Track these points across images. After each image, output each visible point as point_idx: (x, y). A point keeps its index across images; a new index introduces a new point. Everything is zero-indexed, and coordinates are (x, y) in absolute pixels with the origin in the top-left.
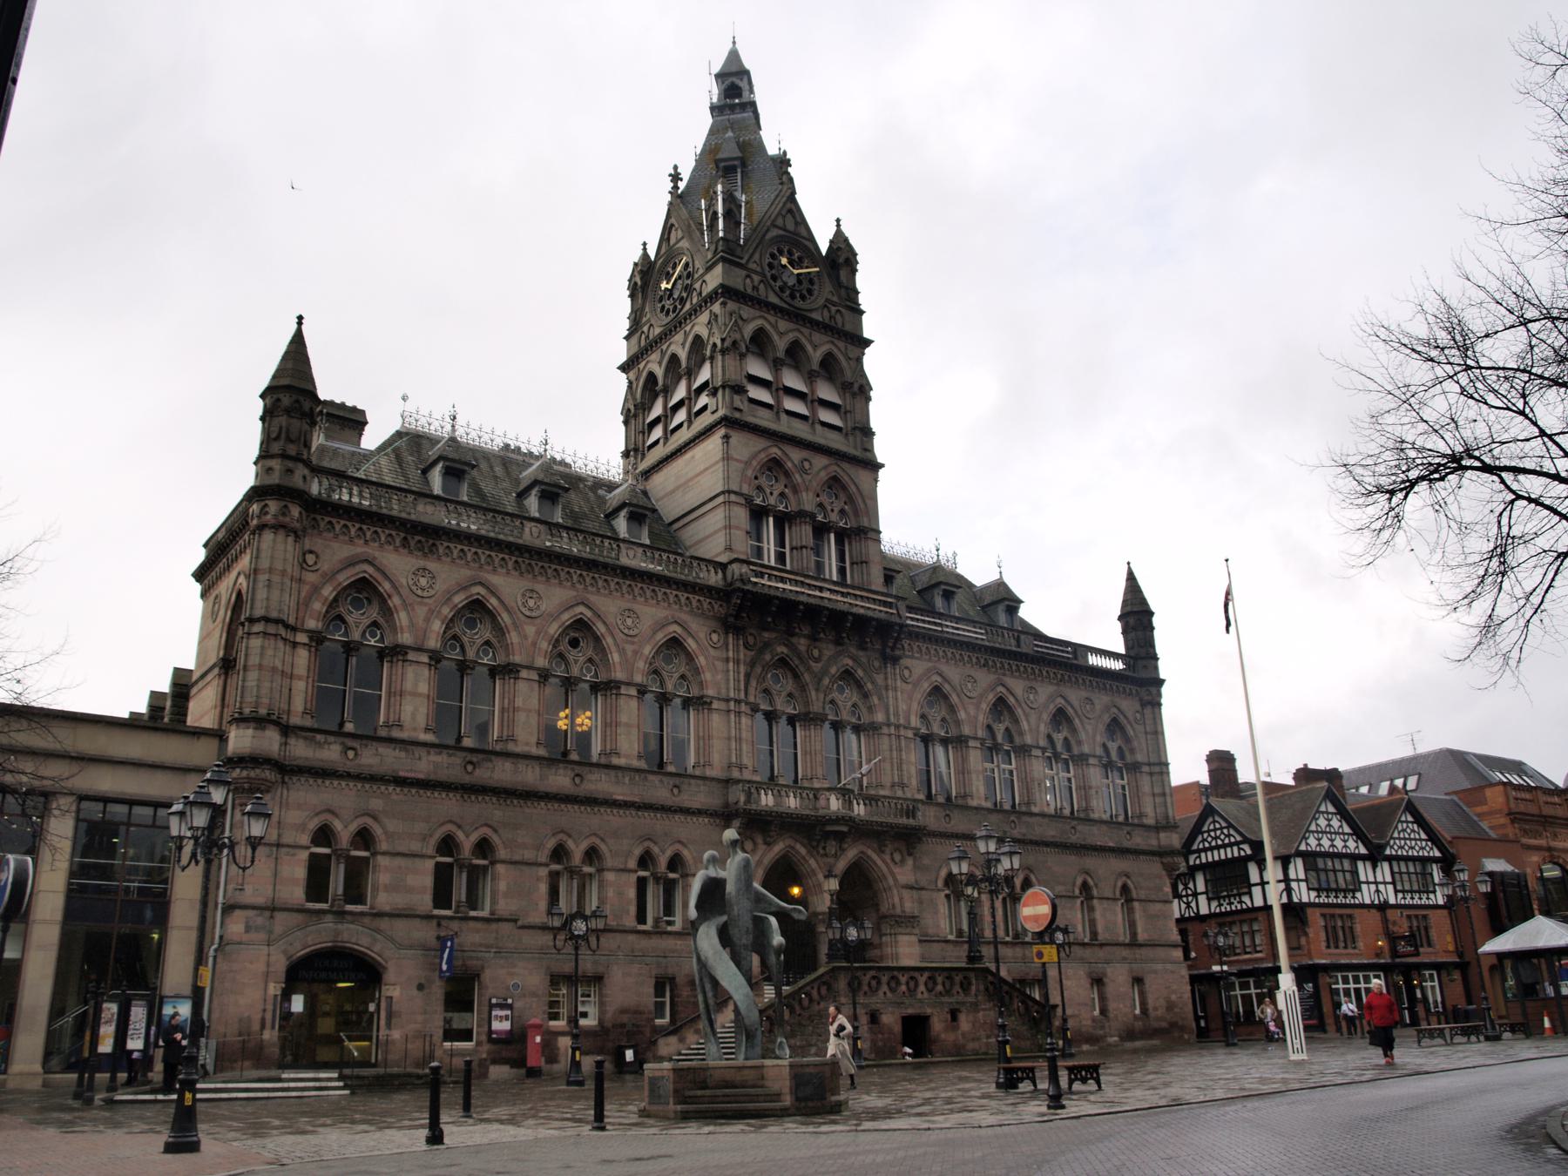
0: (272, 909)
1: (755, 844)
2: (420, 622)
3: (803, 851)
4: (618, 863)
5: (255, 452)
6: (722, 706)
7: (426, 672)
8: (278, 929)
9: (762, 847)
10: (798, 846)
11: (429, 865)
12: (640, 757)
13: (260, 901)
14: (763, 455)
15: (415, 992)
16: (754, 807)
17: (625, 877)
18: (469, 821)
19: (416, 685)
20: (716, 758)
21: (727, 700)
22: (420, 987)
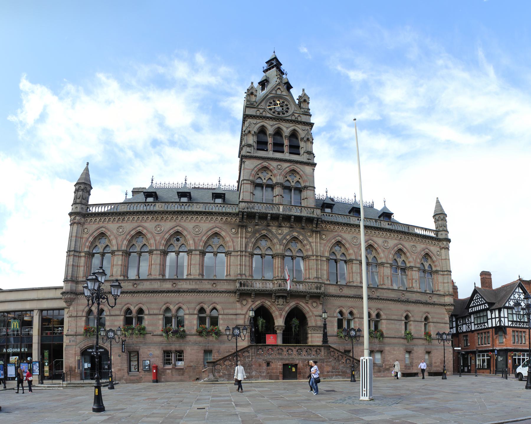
0: (76, 335)
1: (247, 301)
2: (120, 242)
3: (269, 303)
4: (191, 311)
5: (72, 202)
6: (236, 254)
7: (121, 257)
8: (78, 341)
9: (250, 303)
10: (267, 302)
11: (122, 318)
12: (199, 275)
13: (73, 333)
14: (260, 166)
15: (118, 357)
16: (243, 288)
17: (192, 316)
18: (134, 303)
19: (117, 262)
20: (232, 273)
21: (238, 252)
22: (119, 356)
